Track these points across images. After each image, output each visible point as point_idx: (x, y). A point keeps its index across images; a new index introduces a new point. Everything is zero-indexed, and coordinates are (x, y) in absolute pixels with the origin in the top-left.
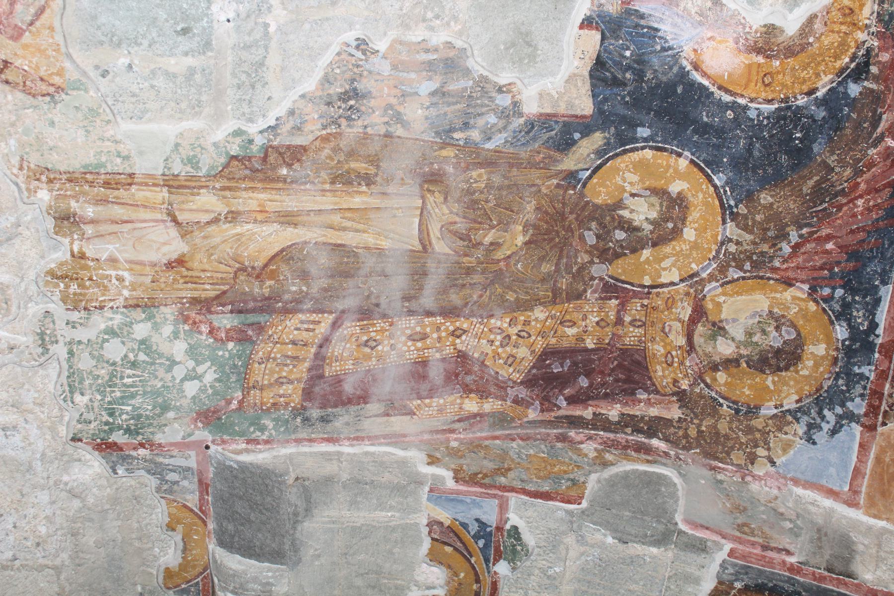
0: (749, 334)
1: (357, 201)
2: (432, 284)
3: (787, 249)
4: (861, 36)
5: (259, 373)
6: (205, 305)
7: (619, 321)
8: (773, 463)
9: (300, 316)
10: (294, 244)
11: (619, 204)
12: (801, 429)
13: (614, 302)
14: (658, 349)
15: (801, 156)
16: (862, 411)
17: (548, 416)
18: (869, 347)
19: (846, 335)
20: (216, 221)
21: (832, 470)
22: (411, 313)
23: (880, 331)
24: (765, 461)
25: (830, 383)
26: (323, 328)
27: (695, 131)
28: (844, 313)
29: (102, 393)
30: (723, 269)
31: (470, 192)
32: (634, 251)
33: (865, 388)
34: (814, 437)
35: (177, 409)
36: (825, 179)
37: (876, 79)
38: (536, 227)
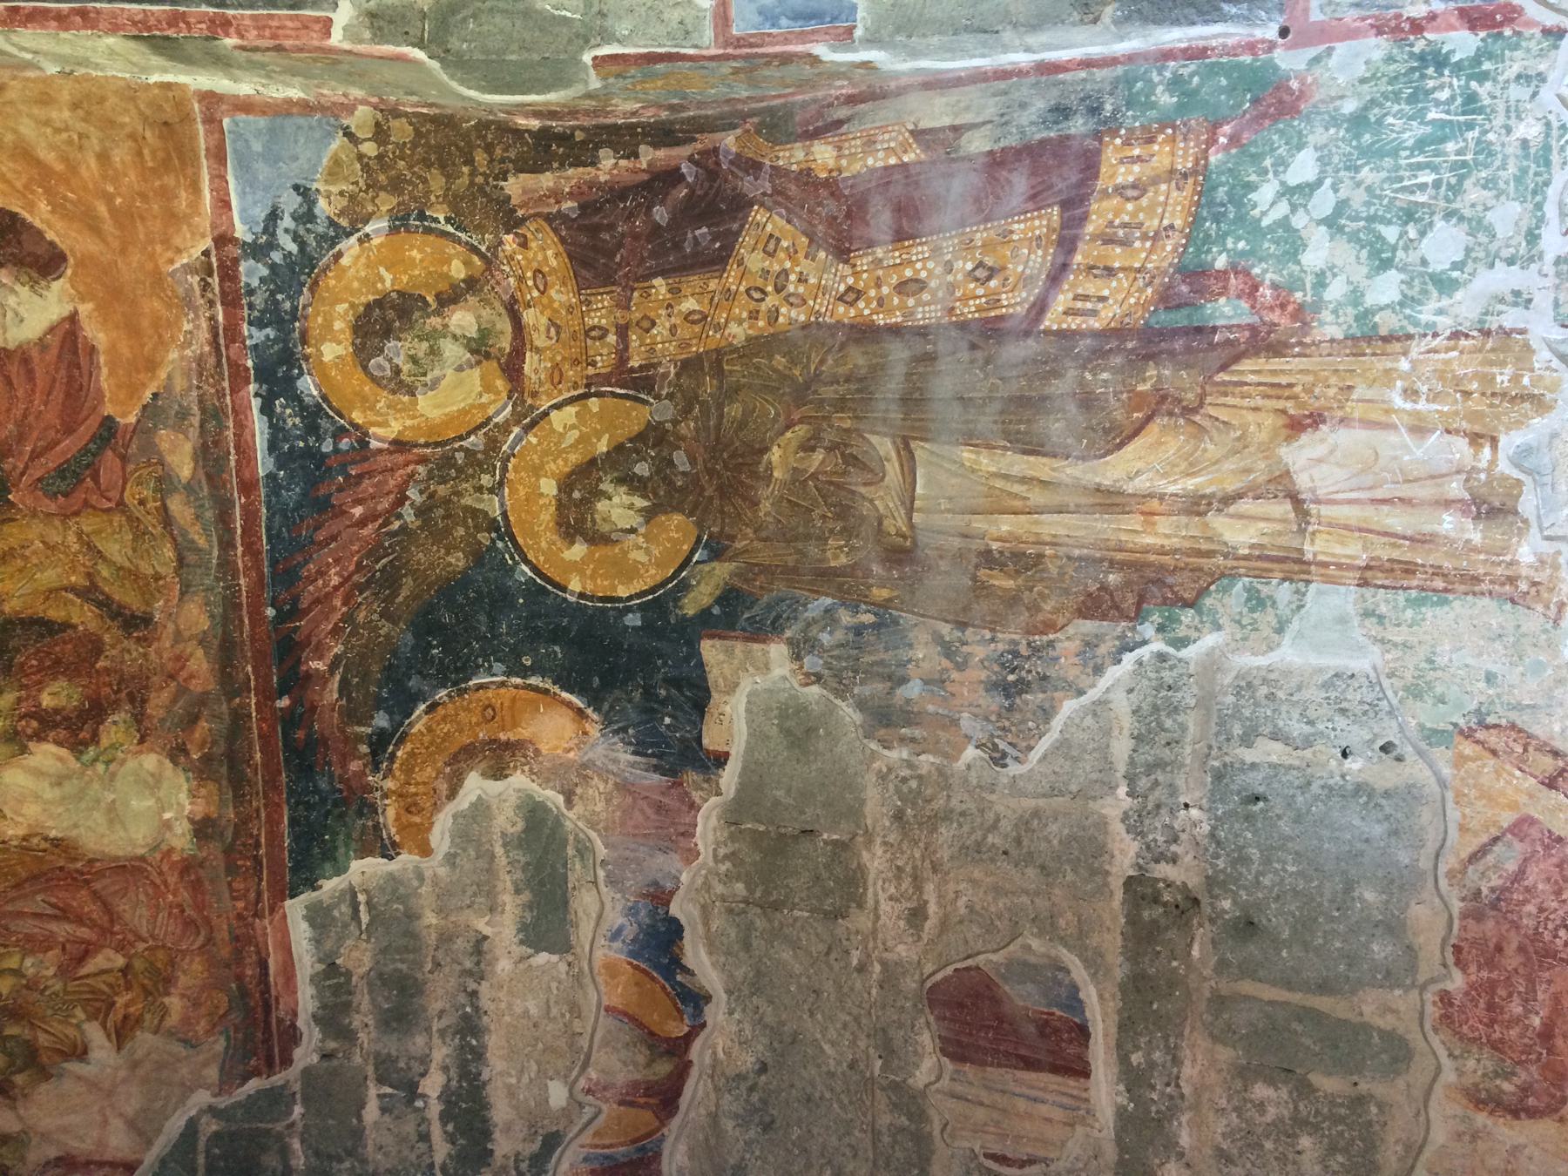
0: (434, 352)
1: (1006, 525)
2: (892, 386)
3: (413, 493)
4: (389, 784)
5: (1173, 205)
6: (1263, 342)
7: (623, 331)
8: (348, 134)
9: (1096, 324)
10: (1104, 456)
11: (649, 515)
12: (323, 207)
13: (635, 363)
14: (561, 295)
15: (425, 625)
16: (243, 267)
17: (704, 141)
18: (263, 374)
19: (299, 383)
20: (1228, 500)
21: (257, 146)
22: (923, 332)
23: (256, 404)
24: (360, 135)
25: (302, 300)
26: (1061, 301)
27: (566, 630)
28: (312, 416)
29: (1484, 148)
30: (493, 444)
31: (848, 533)
32: (619, 448)
33: (251, 306)
34: (299, 199)
35: (1334, 121)
36: (389, 600)
37: (359, 739)
38: (755, 475)
